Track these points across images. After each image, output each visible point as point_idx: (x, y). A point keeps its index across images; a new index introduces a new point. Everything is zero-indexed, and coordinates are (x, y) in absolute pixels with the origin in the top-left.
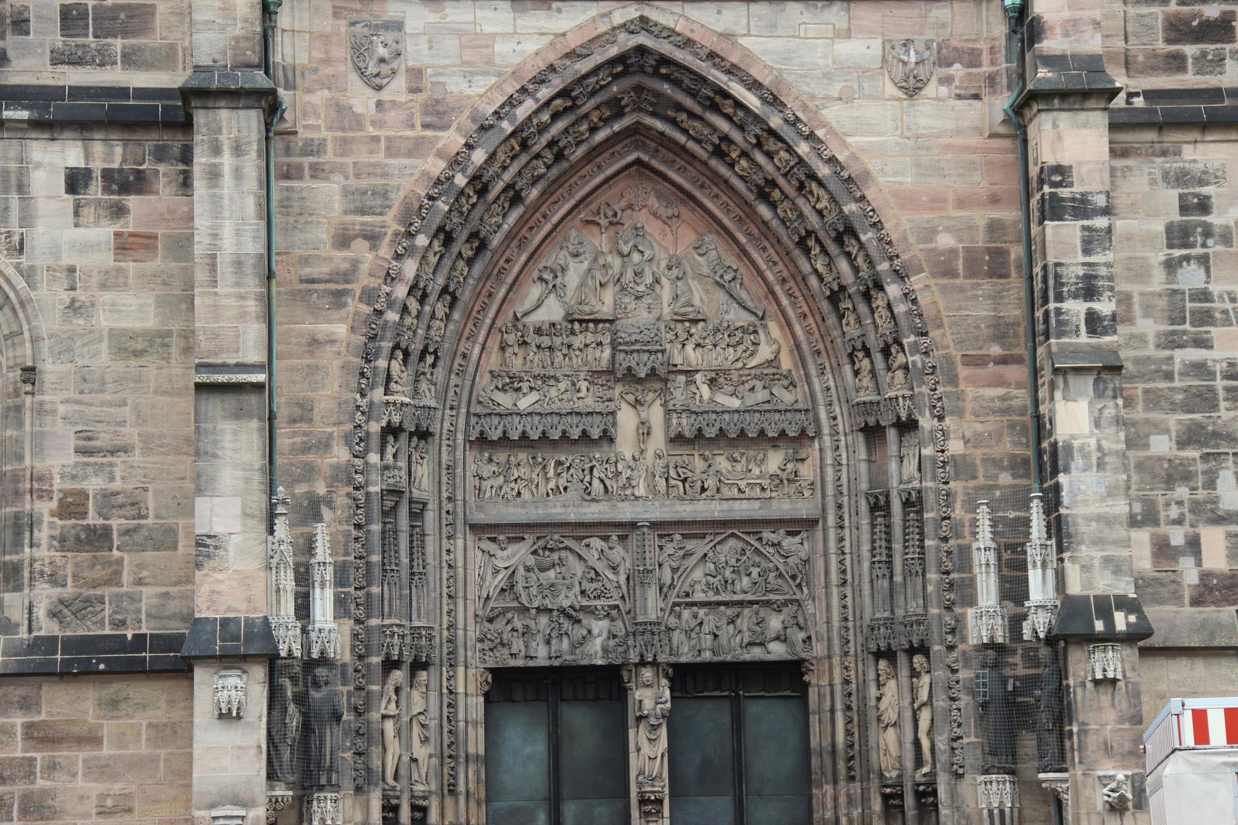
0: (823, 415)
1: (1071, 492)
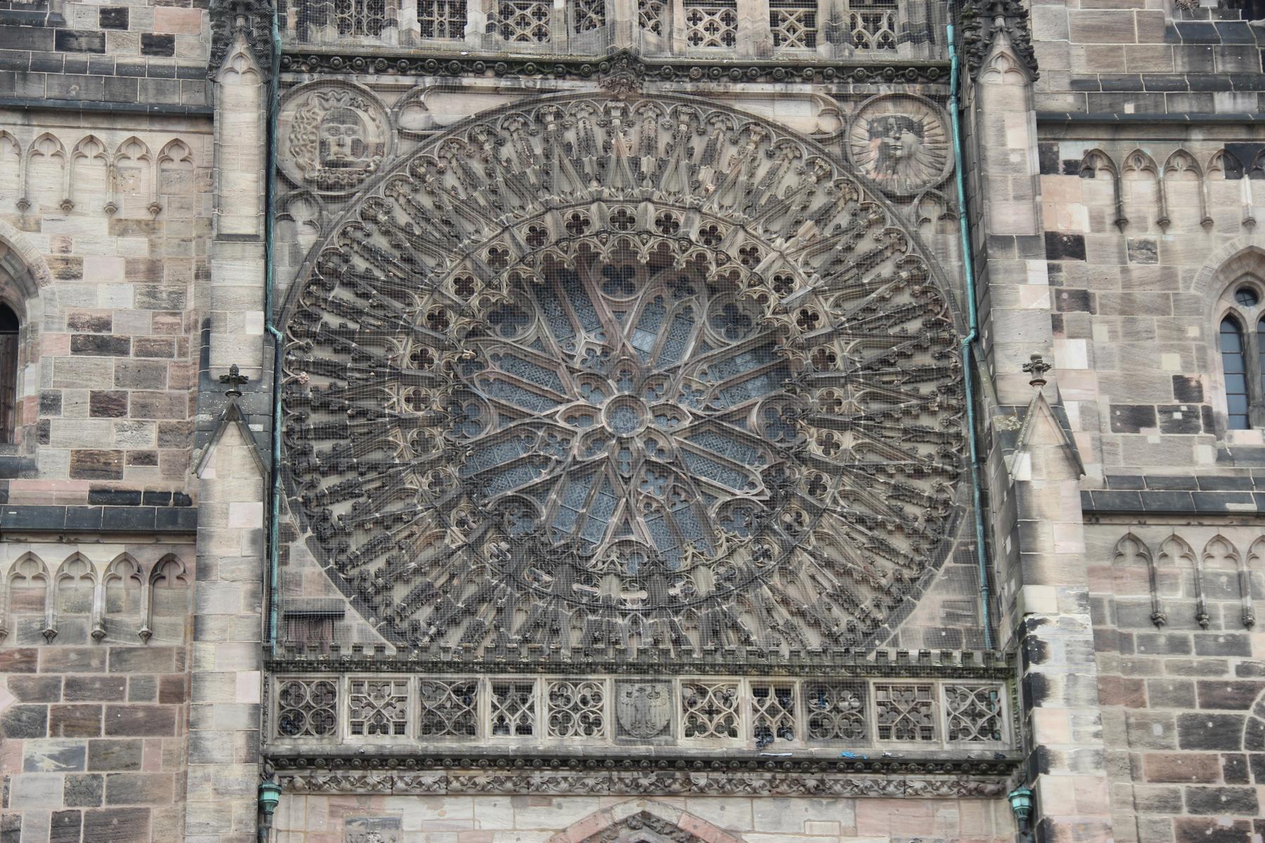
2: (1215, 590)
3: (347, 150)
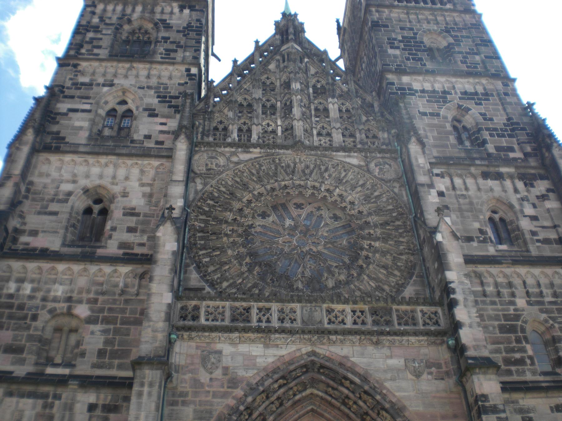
2: (503, 287)
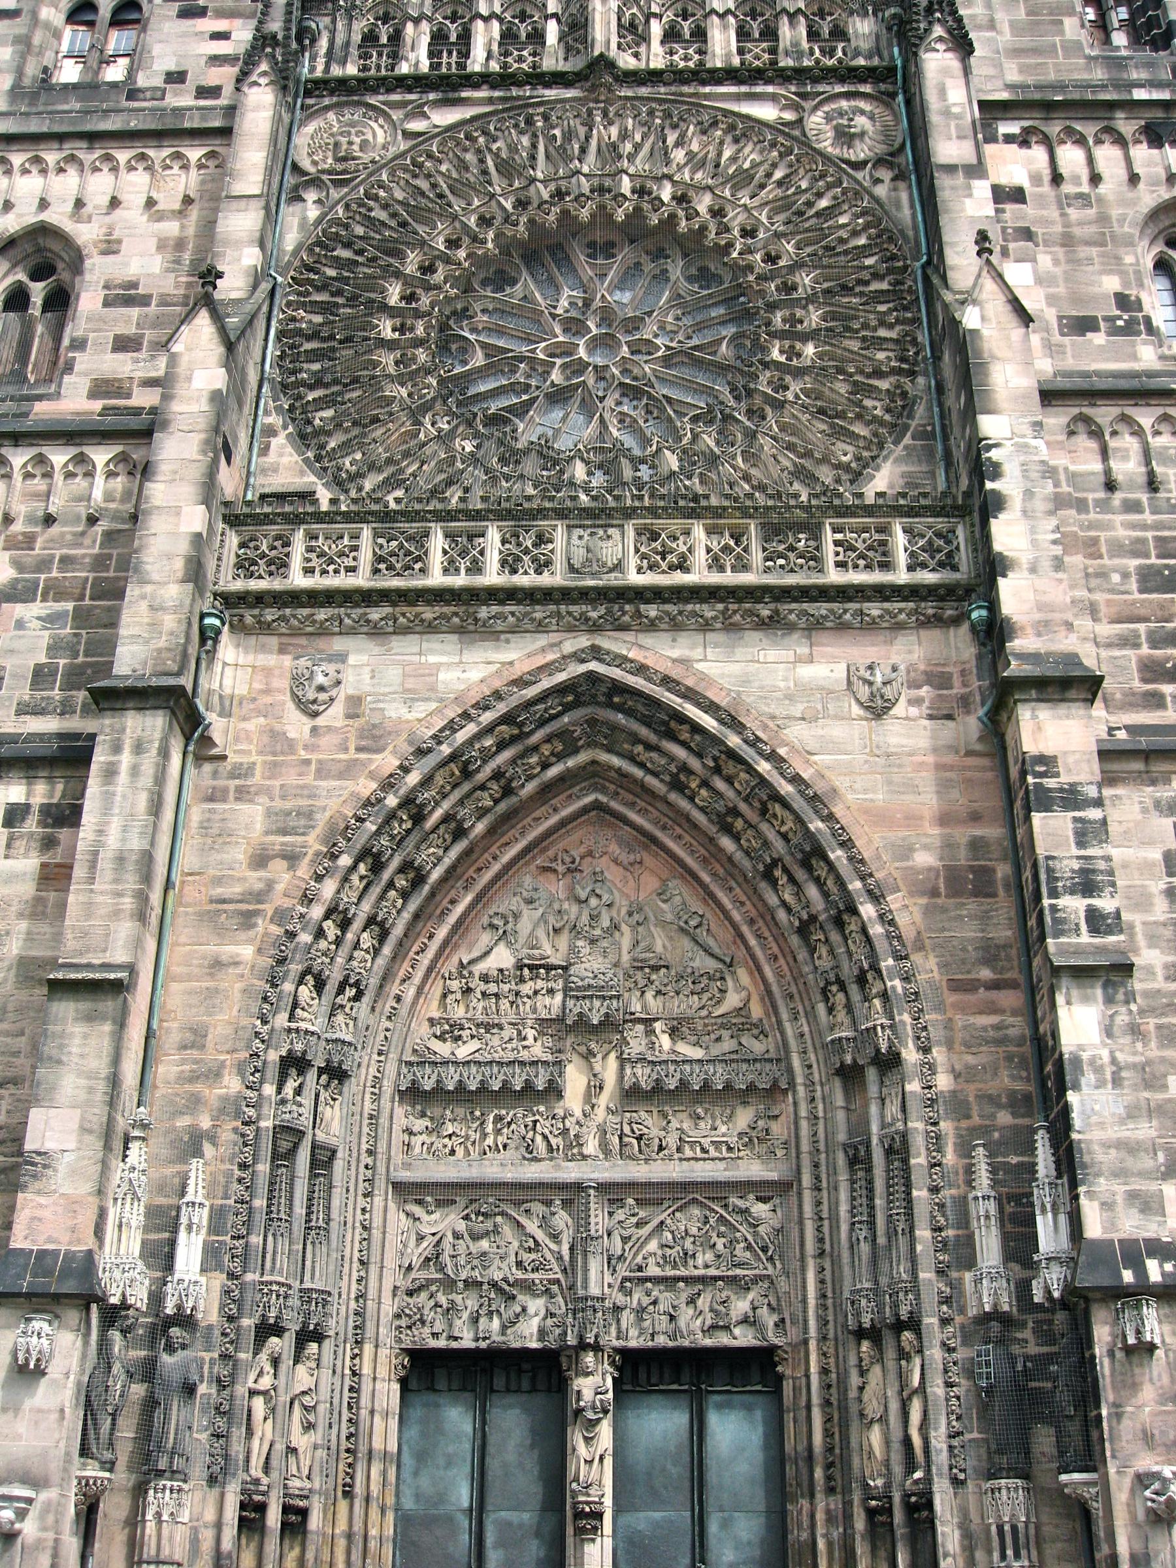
0: (796, 1062)
1: (1083, 1112)
3: (356, 147)
